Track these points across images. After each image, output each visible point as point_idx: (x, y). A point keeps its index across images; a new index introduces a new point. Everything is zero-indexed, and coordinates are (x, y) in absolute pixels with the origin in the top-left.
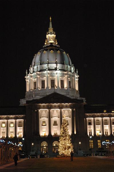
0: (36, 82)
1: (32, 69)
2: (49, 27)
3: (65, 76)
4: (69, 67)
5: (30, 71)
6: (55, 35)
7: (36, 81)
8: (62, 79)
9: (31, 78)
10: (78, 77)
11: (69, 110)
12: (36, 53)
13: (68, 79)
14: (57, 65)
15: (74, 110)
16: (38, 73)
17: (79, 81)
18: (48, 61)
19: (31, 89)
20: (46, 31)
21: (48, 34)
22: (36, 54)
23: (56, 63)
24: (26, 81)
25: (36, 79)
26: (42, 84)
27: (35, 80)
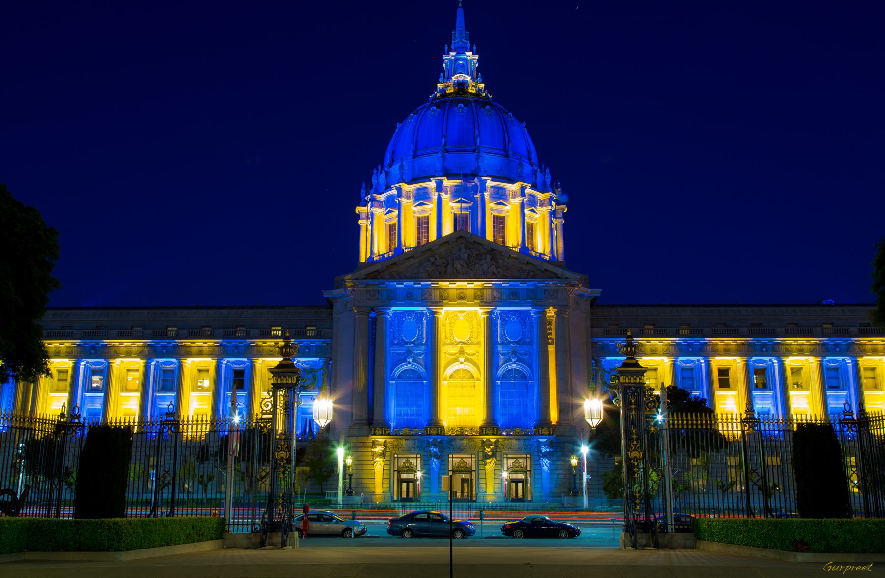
0: (395, 224)
1: (383, 177)
2: (454, 29)
3: (511, 200)
4: (527, 168)
5: (374, 182)
6: (477, 57)
7: (395, 221)
8: (498, 211)
9: (378, 212)
10: (565, 216)
11: (527, 313)
12: (402, 118)
13: (523, 215)
14: (478, 157)
15: (551, 312)
16: (406, 187)
17: (565, 227)
18: (443, 141)
19: (375, 251)
20: (444, 43)
21: (450, 50)
22: (401, 122)
23: (474, 151)
24: (359, 226)
25: (396, 213)
26: (419, 233)
27: (390, 219)
